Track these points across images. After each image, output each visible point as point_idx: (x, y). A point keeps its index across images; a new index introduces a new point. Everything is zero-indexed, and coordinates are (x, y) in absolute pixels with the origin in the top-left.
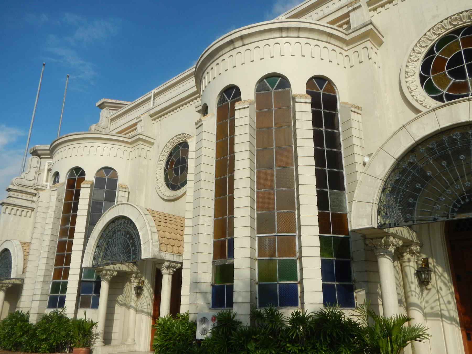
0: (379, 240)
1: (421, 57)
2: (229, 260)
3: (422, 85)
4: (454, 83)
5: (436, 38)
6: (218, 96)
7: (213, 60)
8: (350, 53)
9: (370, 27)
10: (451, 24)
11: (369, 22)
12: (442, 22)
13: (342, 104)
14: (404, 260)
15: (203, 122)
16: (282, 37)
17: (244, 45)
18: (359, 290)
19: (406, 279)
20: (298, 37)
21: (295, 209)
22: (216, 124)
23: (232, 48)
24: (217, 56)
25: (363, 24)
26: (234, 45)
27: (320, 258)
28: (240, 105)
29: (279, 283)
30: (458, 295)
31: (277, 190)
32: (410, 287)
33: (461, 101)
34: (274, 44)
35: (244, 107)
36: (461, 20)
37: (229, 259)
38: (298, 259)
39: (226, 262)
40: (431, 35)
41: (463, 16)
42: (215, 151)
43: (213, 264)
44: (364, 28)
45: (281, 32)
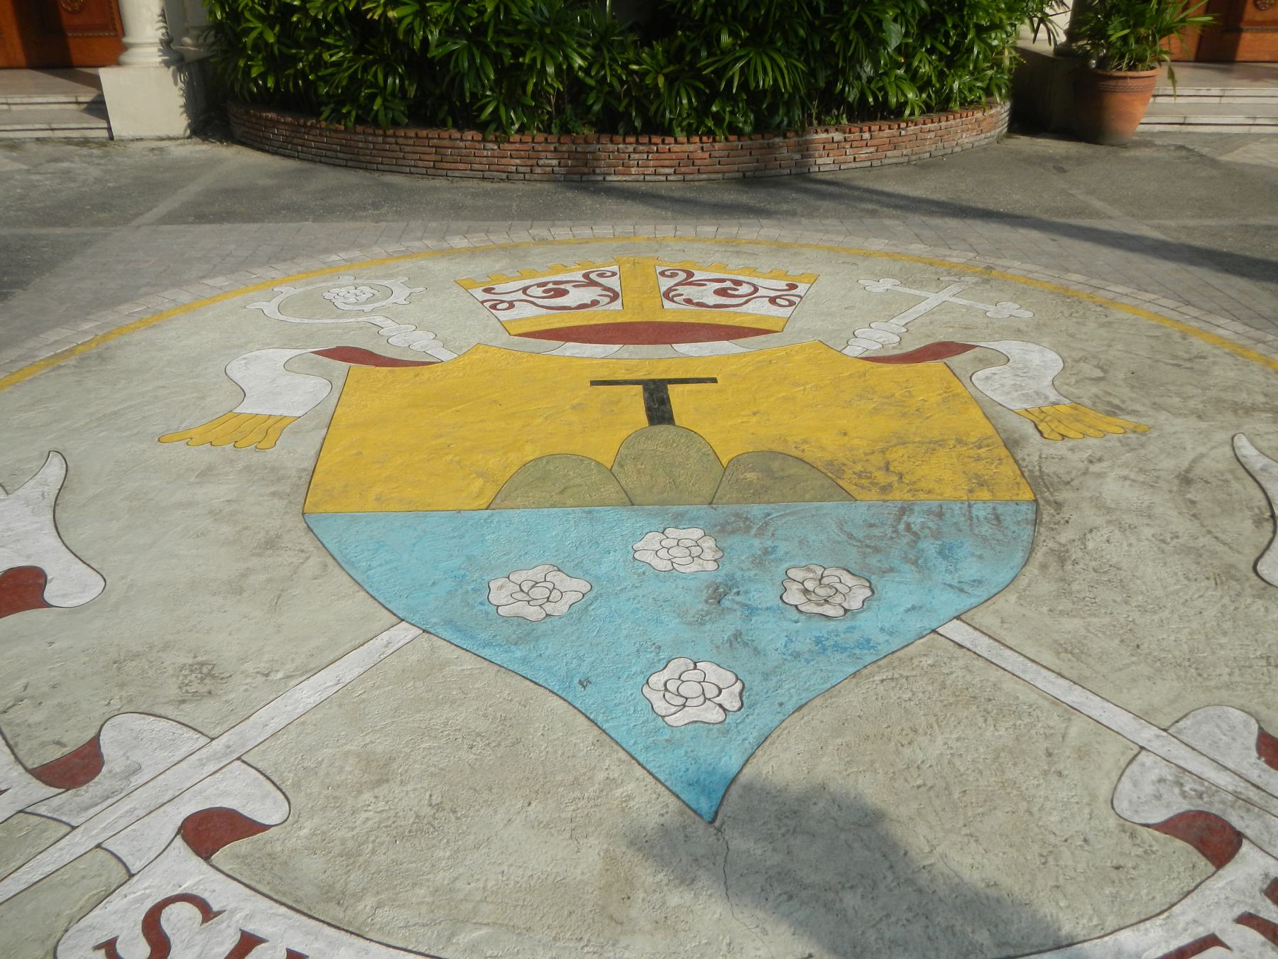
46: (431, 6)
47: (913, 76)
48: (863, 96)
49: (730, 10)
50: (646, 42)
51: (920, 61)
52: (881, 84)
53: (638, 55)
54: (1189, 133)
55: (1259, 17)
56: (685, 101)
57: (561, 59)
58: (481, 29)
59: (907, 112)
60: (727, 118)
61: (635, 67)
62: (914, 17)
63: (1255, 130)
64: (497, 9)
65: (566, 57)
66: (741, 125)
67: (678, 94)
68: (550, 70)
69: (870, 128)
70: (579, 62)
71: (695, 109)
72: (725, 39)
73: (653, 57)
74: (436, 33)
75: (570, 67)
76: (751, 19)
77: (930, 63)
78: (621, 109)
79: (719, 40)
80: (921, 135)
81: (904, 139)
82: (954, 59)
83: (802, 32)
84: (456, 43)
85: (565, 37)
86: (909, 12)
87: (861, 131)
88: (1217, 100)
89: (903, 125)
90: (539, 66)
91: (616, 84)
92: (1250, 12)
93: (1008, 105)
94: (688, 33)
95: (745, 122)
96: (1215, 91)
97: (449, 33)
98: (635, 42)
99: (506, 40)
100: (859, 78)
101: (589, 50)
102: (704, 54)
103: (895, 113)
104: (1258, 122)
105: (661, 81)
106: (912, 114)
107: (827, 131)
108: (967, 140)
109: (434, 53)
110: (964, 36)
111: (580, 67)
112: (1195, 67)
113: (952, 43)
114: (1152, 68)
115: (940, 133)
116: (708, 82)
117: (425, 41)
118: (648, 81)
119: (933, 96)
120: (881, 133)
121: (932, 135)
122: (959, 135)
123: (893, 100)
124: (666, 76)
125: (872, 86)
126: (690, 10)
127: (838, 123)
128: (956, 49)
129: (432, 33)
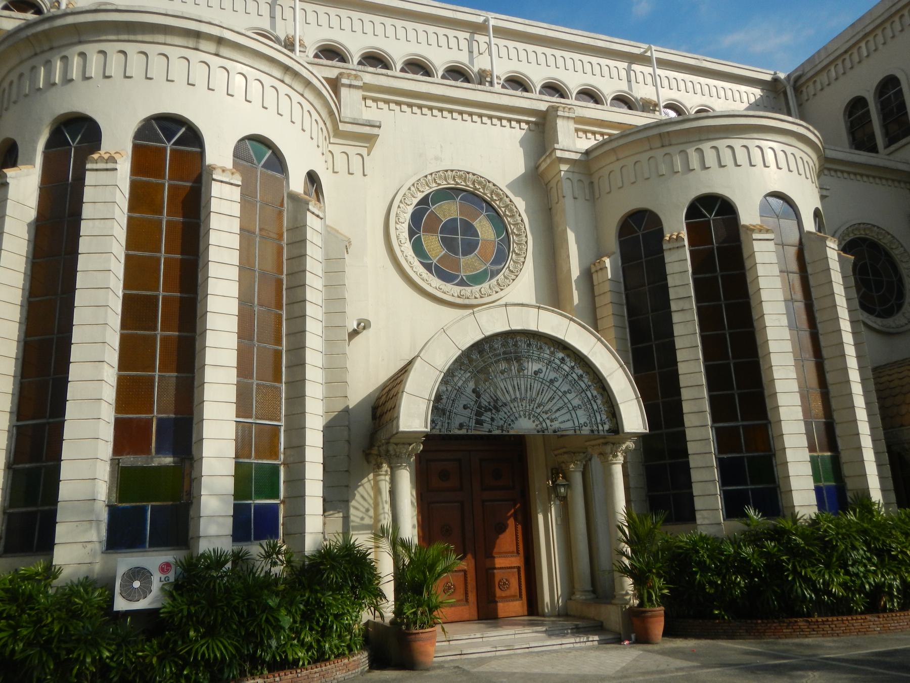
0: (406, 446)
1: (415, 201)
2: (160, 457)
3: (410, 241)
4: (444, 255)
5: (435, 187)
6: (141, 122)
7: (132, 37)
8: (337, 149)
9: (375, 131)
10: (454, 180)
11: (378, 124)
12: (447, 171)
13: (329, 229)
14: (381, 473)
15: (118, 166)
16: (282, 81)
17: (217, 55)
18: (331, 512)
19: (379, 498)
20: (302, 95)
21: (281, 382)
22: (130, 178)
23: (190, 46)
24: (147, 38)
25: (369, 121)
26: (198, 42)
27: (233, 461)
28: (224, 174)
29: (256, 502)
30: (420, 517)
31: (258, 345)
32: (383, 508)
33: (556, 312)
34: (256, 80)
35: (232, 181)
36: (465, 181)
37: (159, 455)
38: (281, 464)
39: (152, 462)
40: (431, 181)
41: (469, 178)
42: (125, 234)
43: (111, 465)
44: (368, 128)
45: (285, 73)
46: (20, 631)
47: (302, 644)
48: (274, 657)
49: (194, 619)
50: (149, 640)
51: (305, 635)
52: (284, 649)
53: (143, 647)
54: (466, 659)
55: (504, 594)
56: (168, 670)
57: (96, 653)
58: (49, 641)
59: (301, 663)
60: (193, 677)
61: (140, 654)
62: (296, 613)
63: (498, 653)
64: (61, 629)
65: (100, 652)
66: (201, 680)
67: (164, 666)
68: (88, 660)
69: (279, 675)
70: (106, 654)
71: (175, 673)
72: (192, 633)
73: (151, 647)
74: (21, 645)
75: (101, 657)
76: (206, 622)
77: (311, 636)
78: (130, 678)
79: (188, 635)
80: (311, 676)
81: (300, 679)
82: (325, 632)
83: (234, 626)
84: (32, 650)
85: (99, 640)
86: (294, 610)
87: (274, 677)
88: (481, 640)
89: (299, 671)
90: (81, 658)
91: (128, 665)
92: (499, 593)
93: (366, 654)
94: (172, 632)
95: (204, 678)
96: (478, 635)
97: (29, 644)
98: (142, 640)
99: (63, 646)
100: (271, 647)
101: (114, 647)
102: (180, 643)
103: (294, 664)
104: (498, 649)
105: (154, 660)
106: (303, 664)
107: (254, 679)
108: (340, 676)
109: (17, 657)
110: (327, 620)
111: (107, 657)
112: (479, 623)
113: (321, 624)
114: (432, 627)
115: (322, 673)
116: (182, 658)
117: (13, 651)
118: (147, 661)
119: (315, 653)
120: (286, 677)
121: (317, 675)
122: (334, 674)
123: (291, 658)
124: (158, 657)
125: (279, 651)
126: (174, 620)
127: (262, 673)
128: (324, 627)
129: (18, 645)
